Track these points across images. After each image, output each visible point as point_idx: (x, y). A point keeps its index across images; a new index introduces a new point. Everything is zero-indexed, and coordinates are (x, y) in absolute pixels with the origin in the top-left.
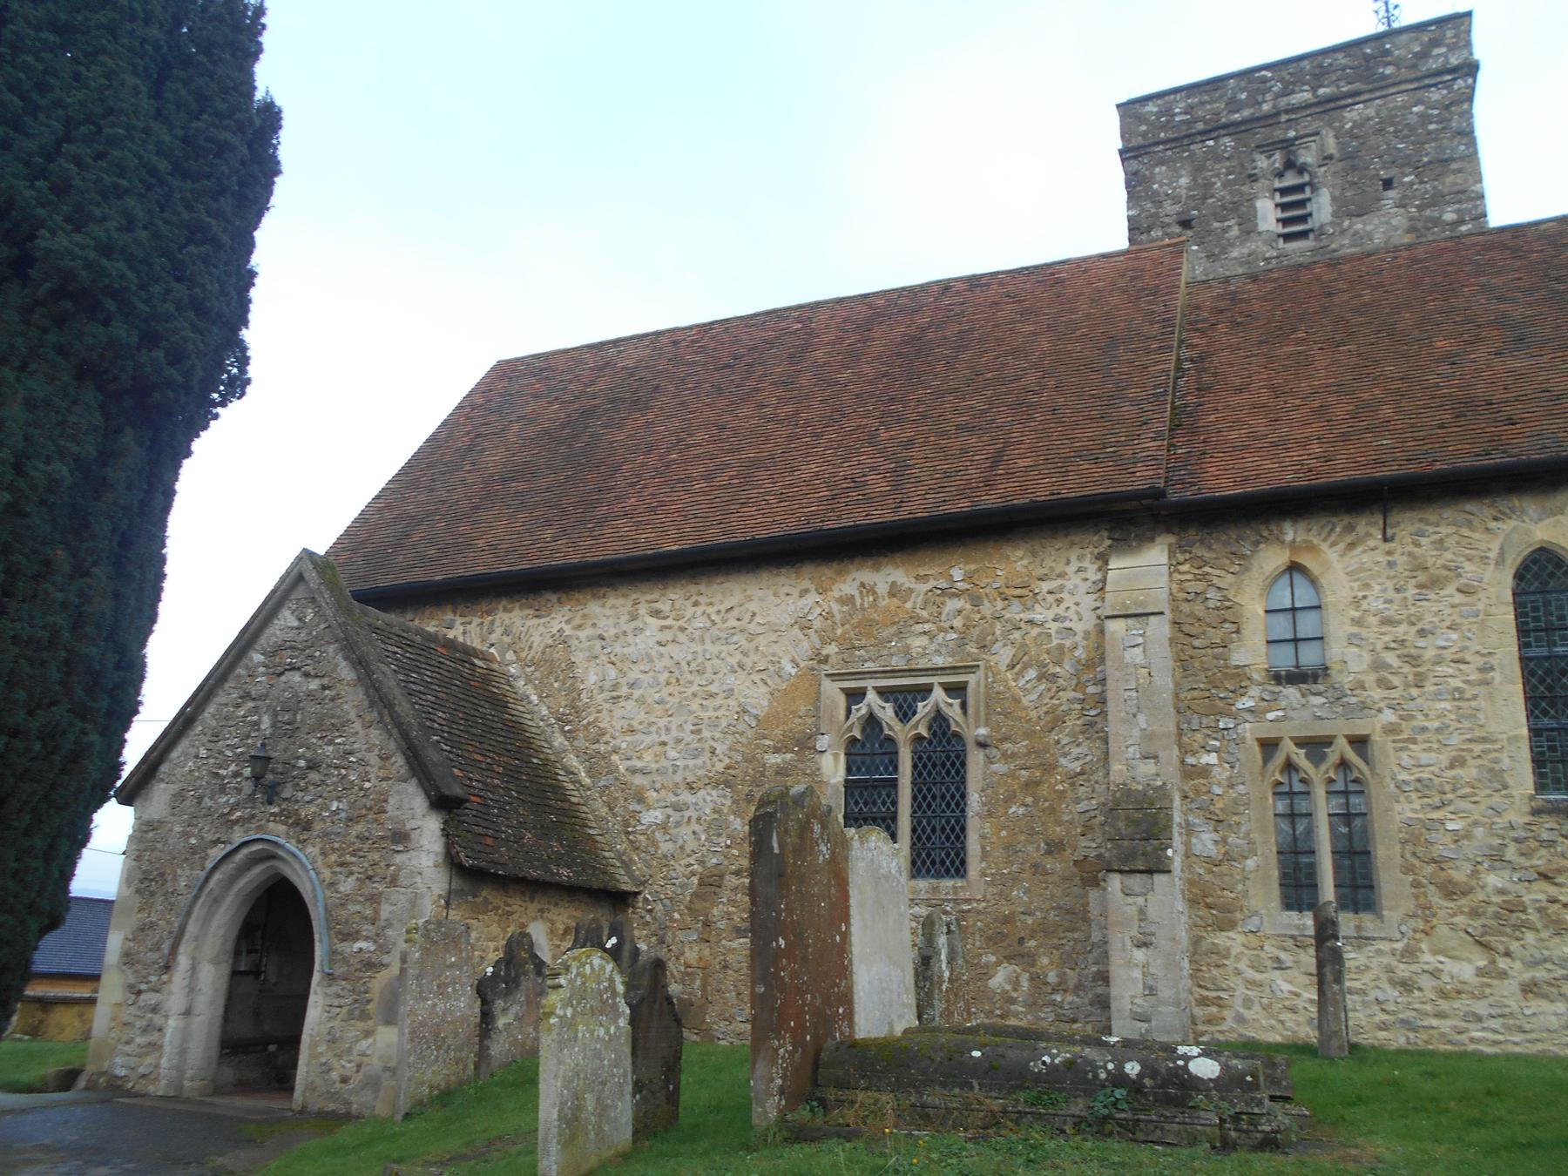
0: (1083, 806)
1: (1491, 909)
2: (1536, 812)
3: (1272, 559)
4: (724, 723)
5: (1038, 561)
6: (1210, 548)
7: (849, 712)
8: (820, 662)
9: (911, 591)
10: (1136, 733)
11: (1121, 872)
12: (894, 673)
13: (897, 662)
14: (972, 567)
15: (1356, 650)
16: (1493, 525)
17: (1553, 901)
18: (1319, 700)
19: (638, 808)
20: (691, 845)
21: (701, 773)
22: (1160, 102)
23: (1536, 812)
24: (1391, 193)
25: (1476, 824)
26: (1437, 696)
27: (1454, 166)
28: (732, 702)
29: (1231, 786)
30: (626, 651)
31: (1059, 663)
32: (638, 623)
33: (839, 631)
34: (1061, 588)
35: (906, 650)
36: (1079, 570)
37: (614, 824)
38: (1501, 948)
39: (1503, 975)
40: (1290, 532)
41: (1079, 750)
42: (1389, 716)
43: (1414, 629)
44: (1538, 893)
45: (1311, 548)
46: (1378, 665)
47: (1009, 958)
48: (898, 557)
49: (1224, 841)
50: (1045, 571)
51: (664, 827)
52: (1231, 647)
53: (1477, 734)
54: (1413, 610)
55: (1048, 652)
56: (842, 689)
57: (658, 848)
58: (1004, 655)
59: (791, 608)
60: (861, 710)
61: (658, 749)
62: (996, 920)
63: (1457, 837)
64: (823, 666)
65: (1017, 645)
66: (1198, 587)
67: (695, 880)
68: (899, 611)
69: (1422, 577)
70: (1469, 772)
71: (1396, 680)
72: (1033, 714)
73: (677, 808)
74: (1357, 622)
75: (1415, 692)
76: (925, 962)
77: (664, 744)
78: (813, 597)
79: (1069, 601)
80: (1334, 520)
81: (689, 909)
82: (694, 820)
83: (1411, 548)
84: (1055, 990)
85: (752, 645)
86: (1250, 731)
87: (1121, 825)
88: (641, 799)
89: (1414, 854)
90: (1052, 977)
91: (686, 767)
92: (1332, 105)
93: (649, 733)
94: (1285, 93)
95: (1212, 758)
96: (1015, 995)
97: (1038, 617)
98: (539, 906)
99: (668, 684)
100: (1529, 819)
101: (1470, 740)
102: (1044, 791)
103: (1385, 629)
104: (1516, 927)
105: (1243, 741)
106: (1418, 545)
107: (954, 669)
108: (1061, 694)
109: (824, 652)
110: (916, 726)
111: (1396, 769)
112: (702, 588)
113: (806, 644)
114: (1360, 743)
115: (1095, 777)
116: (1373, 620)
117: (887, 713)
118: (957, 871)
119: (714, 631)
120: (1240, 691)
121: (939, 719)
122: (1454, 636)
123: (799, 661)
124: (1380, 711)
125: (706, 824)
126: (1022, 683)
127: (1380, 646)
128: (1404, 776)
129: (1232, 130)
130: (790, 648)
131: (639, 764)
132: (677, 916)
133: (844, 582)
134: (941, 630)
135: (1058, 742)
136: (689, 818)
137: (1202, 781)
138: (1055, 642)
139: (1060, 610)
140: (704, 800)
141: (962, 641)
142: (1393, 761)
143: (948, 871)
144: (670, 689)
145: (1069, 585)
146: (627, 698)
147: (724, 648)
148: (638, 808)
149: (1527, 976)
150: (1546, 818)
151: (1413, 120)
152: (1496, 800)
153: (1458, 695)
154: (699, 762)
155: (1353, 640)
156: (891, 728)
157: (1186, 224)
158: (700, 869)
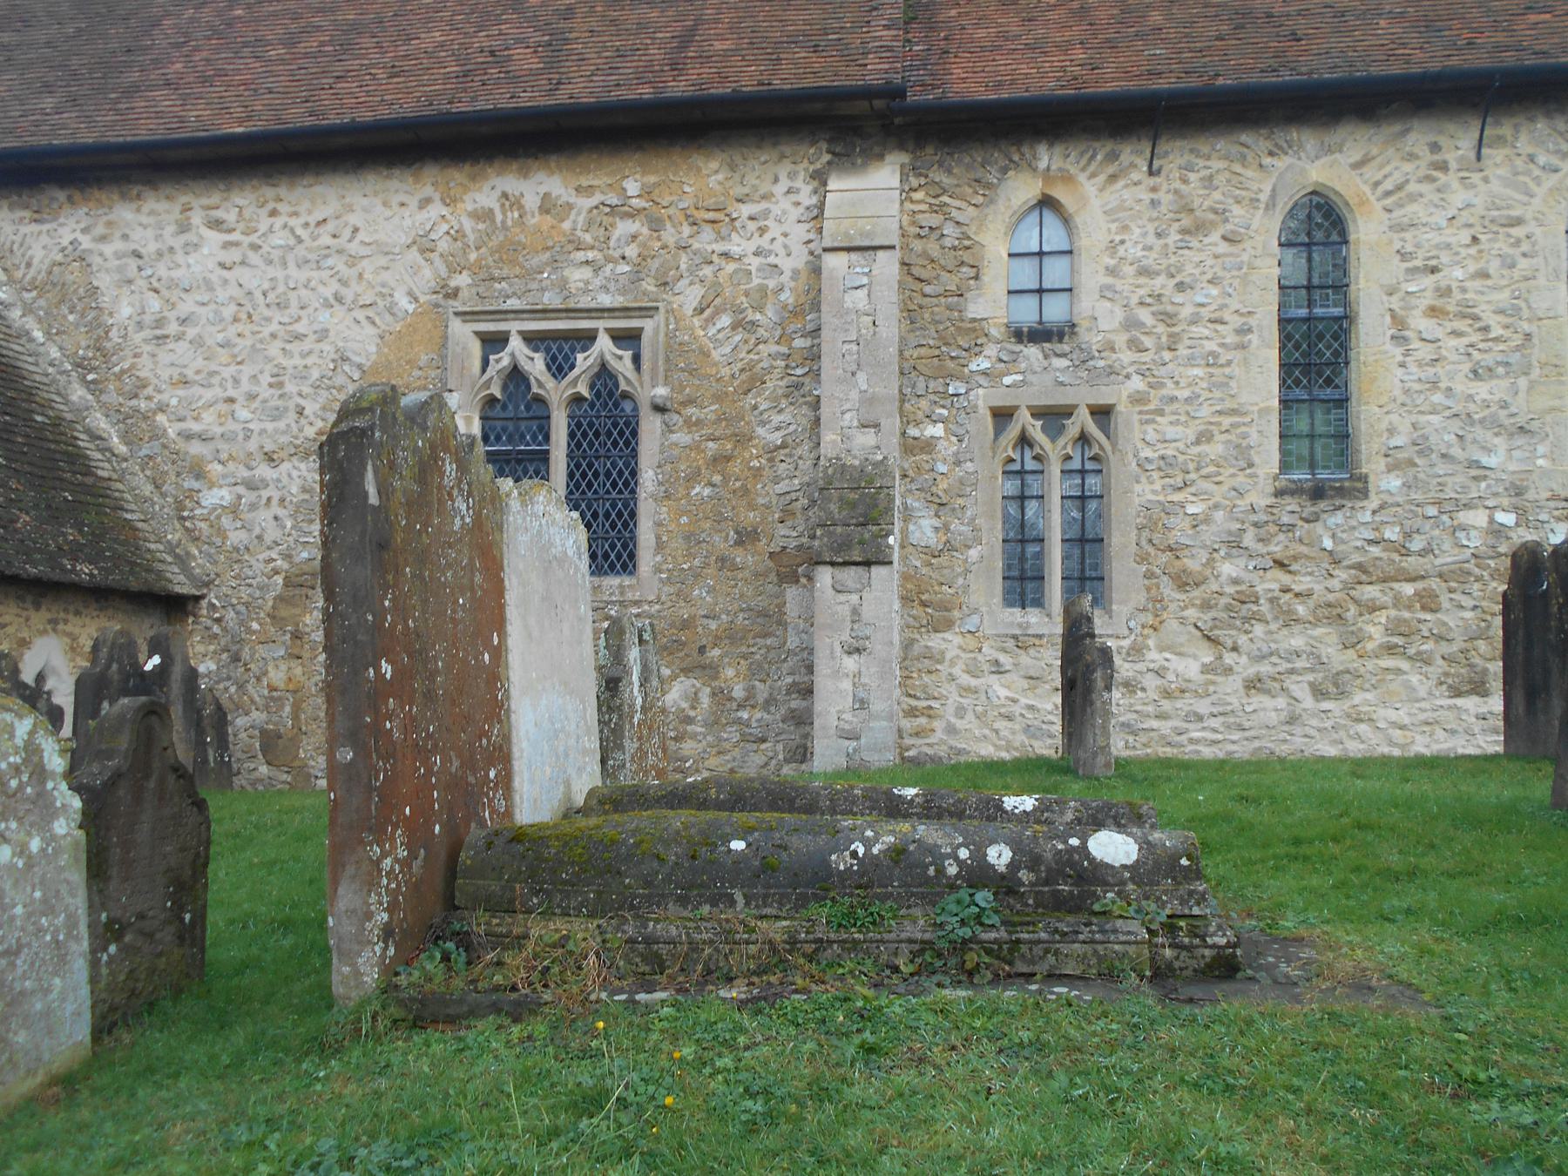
0: (782, 487)
1: (1223, 601)
2: (1279, 493)
3: (1021, 189)
4: (315, 374)
5: (737, 177)
6: (949, 172)
7: (485, 364)
8: (447, 296)
9: (570, 206)
10: (854, 395)
11: (833, 564)
12: (545, 313)
13: (550, 299)
14: (652, 179)
15: (1108, 304)
16: (1267, 161)
17: (1286, 590)
19: (196, 485)
20: (272, 534)
21: (284, 439)
23: (1279, 493)
25: (1216, 506)
26: (1190, 361)
28: (326, 347)
29: (958, 463)
30: (175, 274)
31: (759, 308)
32: (190, 237)
33: (473, 256)
34: (766, 214)
35: (563, 285)
37: (163, 507)
38: (1229, 643)
39: (1229, 671)
40: (1046, 156)
41: (781, 418)
42: (1137, 383)
43: (1173, 282)
44: (1272, 582)
45: (1068, 179)
46: (1131, 324)
47: (686, 671)
48: (553, 160)
49: (946, 527)
50: (746, 190)
51: (234, 510)
52: (968, 295)
53: (1228, 404)
54: (1173, 259)
55: (747, 294)
56: (477, 333)
57: (225, 538)
58: (689, 296)
59: (408, 222)
60: (502, 361)
61: (224, 408)
62: (672, 625)
63: (1196, 522)
64: (451, 302)
65: (707, 284)
66: (935, 220)
67: (279, 580)
68: (554, 232)
69: (1186, 221)
70: (1215, 449)
71: (1148, 342)
72: (725, 372)
73: (251, 486)
74: (1112, 271)
75: (1167, 355)
76: (611, 685)
77: (231, 400)
78: (436, 210)
79: (775, 230)
80: (1097, 145)
81: (272, 617)
82: (275, 502)
83: (1177, 185)
84: (741, 707)
85: (354, 272)
86: (983, 398)
87: (833, 507)
88: (199, 474)
89: (1150, 541)
90: (738, 692)
91: (263, 432)
93: (210, 386)
95: (937, 430)
96: (692, 713)
97: (735, 250)
98: (49, 616)
99: (236, 320)
100: (1271, 500)
101: (1220, 413)
102: (735, 467)
103: (1142, 280)
104: (1246, 620)
105: (975, 409)
106: (1185, 181)
107: (625, 311)
108: (761, 347)
109: (453, 284)
110: (575, 382)
111: (1140, 445)
112: (282, 191)
113: (427, 273)
114: (1102, 413)
115: (799, 451)
116: (1129, 270)
117: (536, 366)
118: (625, 567)
119: (301, 251)
120: (975, 349)
121: (604, 374)
122: (1214, 292)
123: (418, 294)
124: (1128, 377)
125: (291, 507)
126: (712, 331)
127: (1134, 300)
128: (1147, 453)
130: (407, 278)
131: (195, 427)
132: (255, 626)
133: (480, 190)
134: (609, 260)
135: (755, 407)
136: (269, 499)
137: (925, 457)
138: (756, 281)
139: (764, 242)
140: (289, 476)
141: (636, 277)
142: (1137, 435)
143: (612, 567)
144: (240, 327)
145: (776, 210)
146: (178, 338)
147: (315, 274)
148: (196, 485)
149: (1251, 671)
150: (1288, 499)
152: (1241, 480)
153: (1212, 360)
154: (281, 425)
155: (1106, 293)
156: (540, 385)
158: (286, 566)
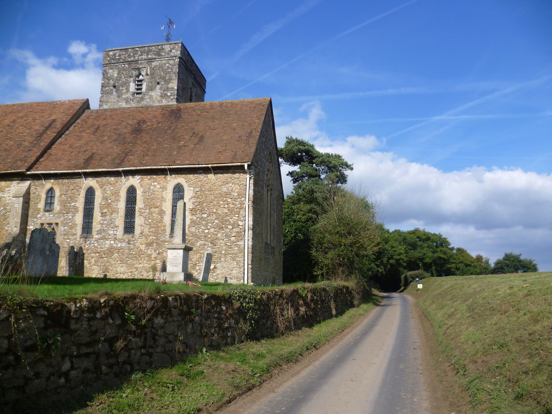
10: (14, 221)
18: (52, 215)
22: (113, 52)
24: (158, 86)
27: (172, 81)
34: (10, 190)
36: (14, 186)
92: (150, 60)
94: (141, 55)
97: (5, 196)
120: (38, 213)
129: (128, 63)
151: (166, 67)
157: (114, 87)
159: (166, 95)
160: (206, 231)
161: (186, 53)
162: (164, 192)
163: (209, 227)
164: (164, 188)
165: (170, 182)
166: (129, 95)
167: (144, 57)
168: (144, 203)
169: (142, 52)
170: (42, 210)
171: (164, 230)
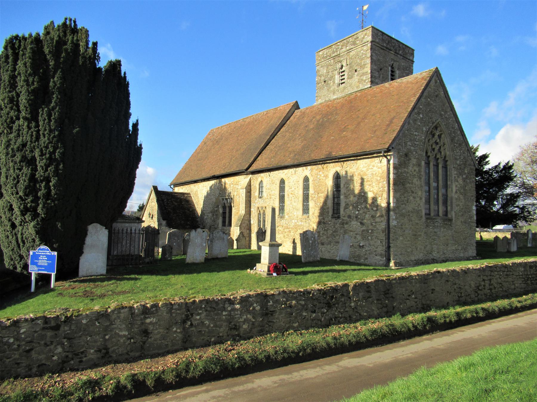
22: (322, 51)
24: (356, 73)
27: (366, 66)
159: (362, 80)
160: (357, 212)
161: (380, 34)
162: (327, 180)
163: (359, 209)
164: (326, 176)
165: (330, 171)
166: (335, 86)
167: (344, 49)
168: (314, 189)
169: (342, 46)
170: (257, 197)
171: (328, 212)
